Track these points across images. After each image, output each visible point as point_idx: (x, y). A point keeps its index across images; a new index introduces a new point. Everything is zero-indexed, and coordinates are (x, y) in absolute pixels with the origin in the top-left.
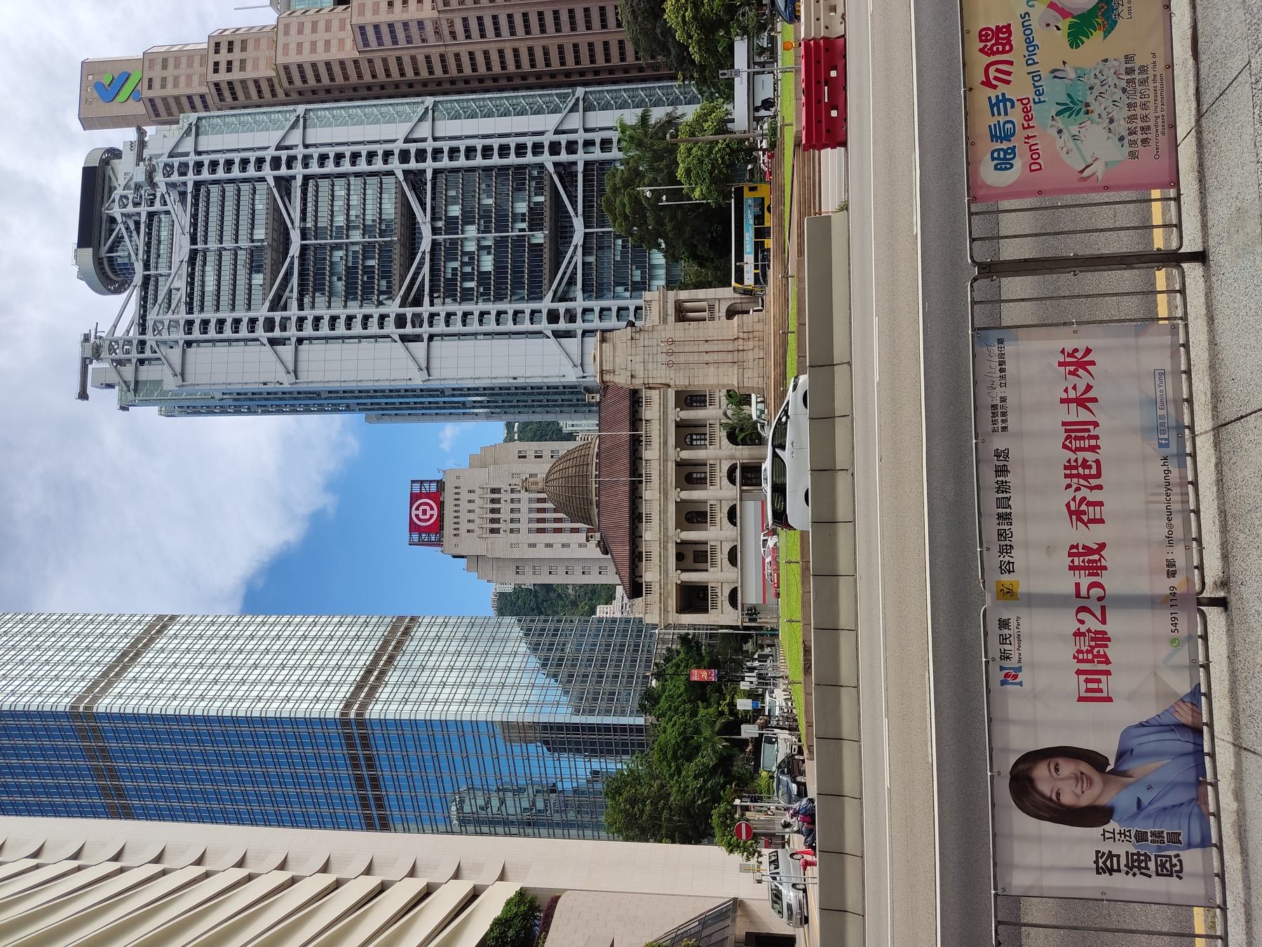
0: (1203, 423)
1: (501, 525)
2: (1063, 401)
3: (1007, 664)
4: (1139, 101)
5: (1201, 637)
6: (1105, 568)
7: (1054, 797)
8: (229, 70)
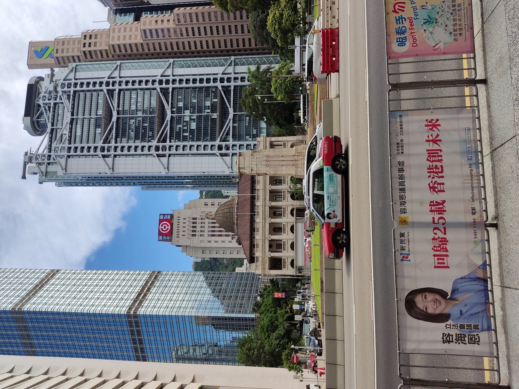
0: (486, 151)
2: (427, 141)
3: (403, 252)
4: (458, 18)
5: (487, 240)
6: (445, 211)
7: (424, 310)
8: (90, 46)
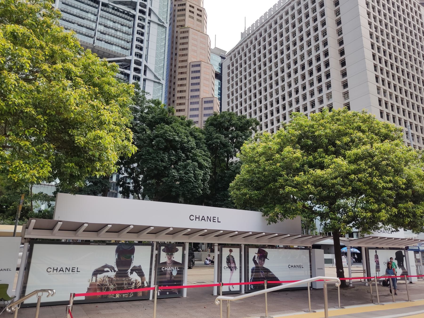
8: (190, 11)
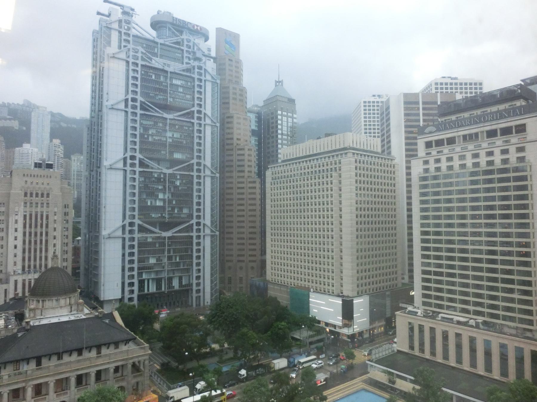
1: (28, 198)
